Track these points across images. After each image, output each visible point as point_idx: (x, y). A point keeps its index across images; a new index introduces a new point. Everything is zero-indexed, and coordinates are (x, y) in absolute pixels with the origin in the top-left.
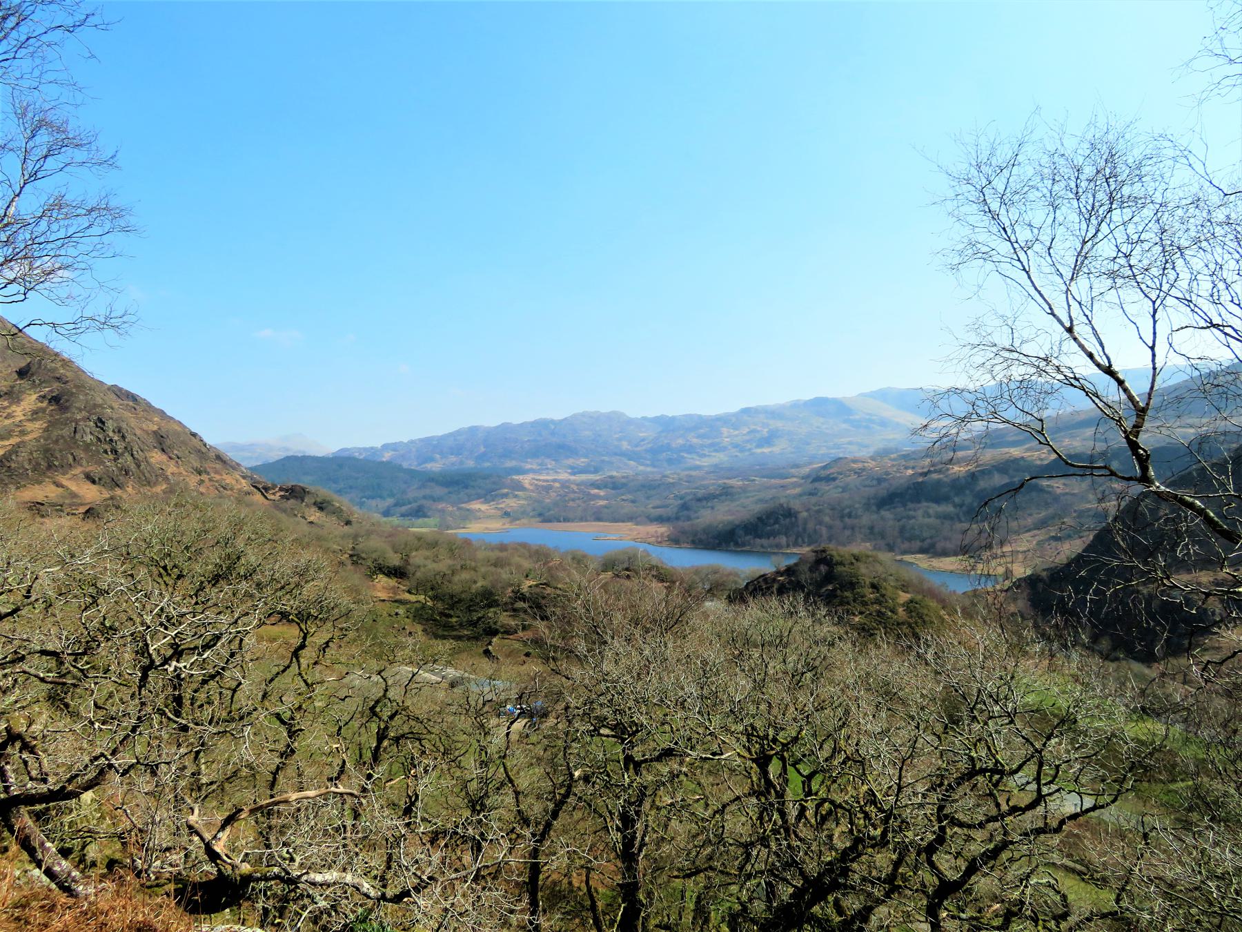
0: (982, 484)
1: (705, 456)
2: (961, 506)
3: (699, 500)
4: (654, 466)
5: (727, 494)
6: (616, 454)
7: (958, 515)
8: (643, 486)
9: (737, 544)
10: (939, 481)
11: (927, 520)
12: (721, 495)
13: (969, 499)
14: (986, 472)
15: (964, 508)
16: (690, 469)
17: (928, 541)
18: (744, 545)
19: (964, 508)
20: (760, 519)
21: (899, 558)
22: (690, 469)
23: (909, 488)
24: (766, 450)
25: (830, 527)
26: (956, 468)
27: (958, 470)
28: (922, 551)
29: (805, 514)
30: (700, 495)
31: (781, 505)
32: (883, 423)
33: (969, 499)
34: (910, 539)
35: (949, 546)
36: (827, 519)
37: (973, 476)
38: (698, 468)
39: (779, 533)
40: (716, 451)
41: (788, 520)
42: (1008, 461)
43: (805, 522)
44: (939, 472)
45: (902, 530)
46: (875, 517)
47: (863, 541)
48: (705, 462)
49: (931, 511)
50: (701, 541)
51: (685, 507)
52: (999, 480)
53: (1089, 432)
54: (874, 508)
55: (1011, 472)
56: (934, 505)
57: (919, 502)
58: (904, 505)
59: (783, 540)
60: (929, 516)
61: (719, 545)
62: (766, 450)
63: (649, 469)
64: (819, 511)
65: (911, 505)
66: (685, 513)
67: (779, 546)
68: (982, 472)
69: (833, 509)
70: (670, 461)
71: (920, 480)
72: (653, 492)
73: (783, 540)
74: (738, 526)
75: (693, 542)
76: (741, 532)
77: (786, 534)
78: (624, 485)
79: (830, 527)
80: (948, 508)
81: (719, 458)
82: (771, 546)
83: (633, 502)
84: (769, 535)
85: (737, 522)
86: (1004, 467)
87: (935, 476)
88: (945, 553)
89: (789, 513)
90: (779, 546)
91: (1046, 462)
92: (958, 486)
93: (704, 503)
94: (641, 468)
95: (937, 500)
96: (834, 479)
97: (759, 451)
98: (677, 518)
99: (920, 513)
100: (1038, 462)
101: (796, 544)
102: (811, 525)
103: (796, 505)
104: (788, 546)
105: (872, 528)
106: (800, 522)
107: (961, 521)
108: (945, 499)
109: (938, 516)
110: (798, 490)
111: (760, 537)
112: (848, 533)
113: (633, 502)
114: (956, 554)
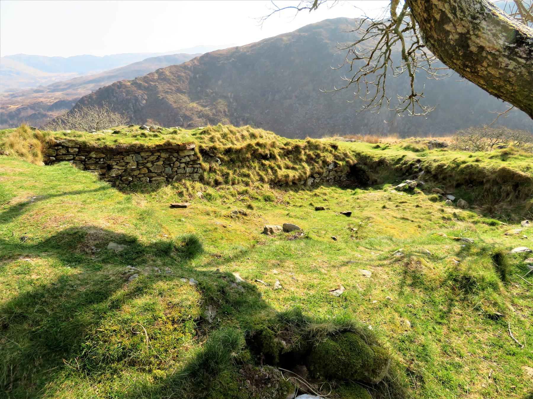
0: (23, 114)
14: (24, 109)
26: (12, 107)
27: (13, 107)
37: (19, 110)
42: (35, 103)
52: (30, 112)
53: (91, 86)
68: (23, 108)
86: (33, 106)
91: (52, 104)
100: (49, 104)
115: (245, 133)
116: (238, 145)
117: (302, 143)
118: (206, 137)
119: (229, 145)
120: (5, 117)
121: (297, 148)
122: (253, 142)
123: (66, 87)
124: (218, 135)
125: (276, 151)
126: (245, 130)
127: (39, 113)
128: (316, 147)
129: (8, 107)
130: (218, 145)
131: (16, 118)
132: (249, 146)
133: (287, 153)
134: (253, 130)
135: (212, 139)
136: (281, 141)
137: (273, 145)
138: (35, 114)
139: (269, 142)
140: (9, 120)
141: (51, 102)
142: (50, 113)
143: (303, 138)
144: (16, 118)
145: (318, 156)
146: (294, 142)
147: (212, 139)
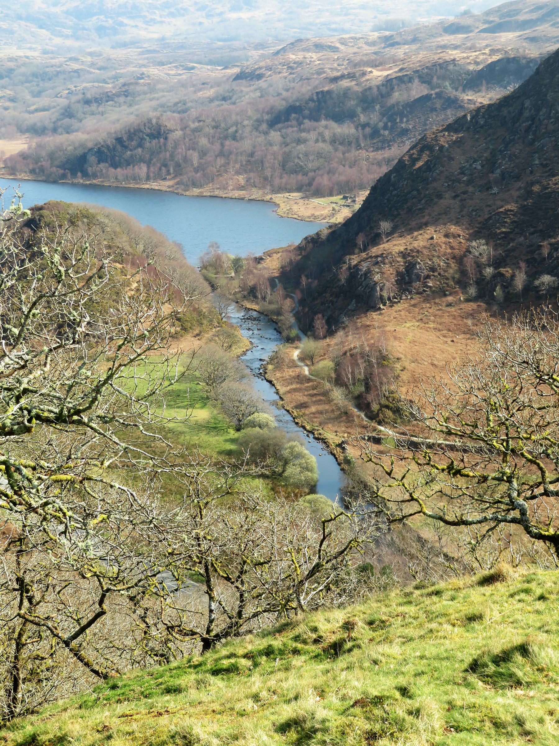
0: (398, 96)
1: (154, 21)
2: (364, 126)
3: (87, 102)
4: (77, 39)
5: (126, 94)
6: (20, 18)
7: (357, 139)
8: (35, 75)
9: (85, 175)
10: (348, 89)
11: (321, 145)
12: (118, 95)
13: (375, 117)
14: (403, 80)
15: (368, 130)
16: (124, 45)
17: (311, 174)
18: (95, 176)
19: (368, 130)
20: (119, 140)
21: (268, 197)
22: (124, 45)
23: (311, 100)
24: (245, 15)
25: (203, 154)
27: (377, 75)
28: (299, 189)
29: (179, 133)
30: (89, 96)
31: (150, 121)
33: (375, 117)
34: (295, 172)
35: (325, 181)
36: (203, 141)
37: (389, 83)
38: (134, 43)
39: (142, 160)
40: (172, 15)
41: (154, 142)
43: (176, 145)
44: (351, 76)
45: (287, 158)
46: (261, 139)
47: (238, 173)
48: (153, 33)
49: (327, 134)
50: (42, 170)
51: (68, 113)
52: (418, 90)
54: (264, 126)
55: (435, 79)
56: (332, 124)
57: (317, 120)
58: (300, 124)
59: (142, 170)
60: (324, 141)
61: (64, 176)
63: (69, 43)
64: (195, 130)
65: (307, 123)
66: (67, 121)
67: (136, 178)
68: (400, 79)
69: (216, 127)
70: (101, 30)
71: (326, 89)
72: (48, 84)
73: (144, 168)
74: (91, 150)
75: (33, 171)
76: (92, 159)
77: (149, 163)
78: (11, 71)
79: (203, 154)
80: (347, 129)
81: (172, 29)
82: (126, 178)
83: (13, 100)
84: (128, 163)
85: (90, 145)
87: (345, 83)
88: (318, 193)
89: (158, 133)
90: (136, 178)
91: (480, 67)
92: (368, 99)
93: (94, 107)
94: (58, 41)
95: (339, 117)
96: (260, 77)
97: (234, 15)
98: (55, 130)
99: (313, 136)
100: (471, 68)
101: (159, 177)
102: (181, 150)
103: (170, 121)
104: (148, 178)
105: (252, 155)
106: (170, 144)
107: (359, 147)
109: (334, 141)
110: (211, 93)
111: (116, 168)
112: (220, 161)
113: (13, 100)
114: (331, 195)
120: (352, 103)
123: (534, 16)
127: (439, 95)
129: (364, 74)
131: (378, 107)
138: (427, 98)
140: (359, 109)
141: (477, 63)
144: (378, 107)
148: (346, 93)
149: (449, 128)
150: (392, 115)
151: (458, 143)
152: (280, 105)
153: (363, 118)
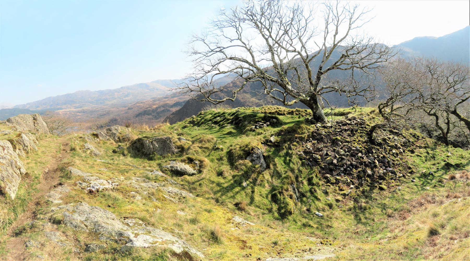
0: (159, 110)
13: (155, 114)
14: (159, 107)
24: (126, 98)
27: (155, 107)
32: (157, 89)
33: (155, 114)
37: (157, 108)
52: (162, 109)
62: (126, 98)
80: (150, 117)
86: (163, 106)
87: (149, 109)
92: (154, 111)
95: (149, 115)
108: (151, 114)
115: (275, 108)
116: (273, 111)
117: (294, 110)
118: (263, 109)
119: (270, 111)
120: (151, 112)
121: (292, 112)
122: (278, 110)
124: (267, 108)
125: (285, 113)
126: (275, 107)
128: (299, 111)
130: (267, 111)
132: (276, 111)
133: (289, 113)
134: (278, 107)
135: (265, 110)
136: (287, 110)
137: (284, 111)
139: (283, 110)
142: (171, 109)
143: (295, 108)
145: (300, 114)
146: (291, 110)
147: (265, 110)
148: (149, 110)
149: (172, 114)
150: (158, 113)
151: (174, 117)
152: (138, 113)
153: (153, 114)
